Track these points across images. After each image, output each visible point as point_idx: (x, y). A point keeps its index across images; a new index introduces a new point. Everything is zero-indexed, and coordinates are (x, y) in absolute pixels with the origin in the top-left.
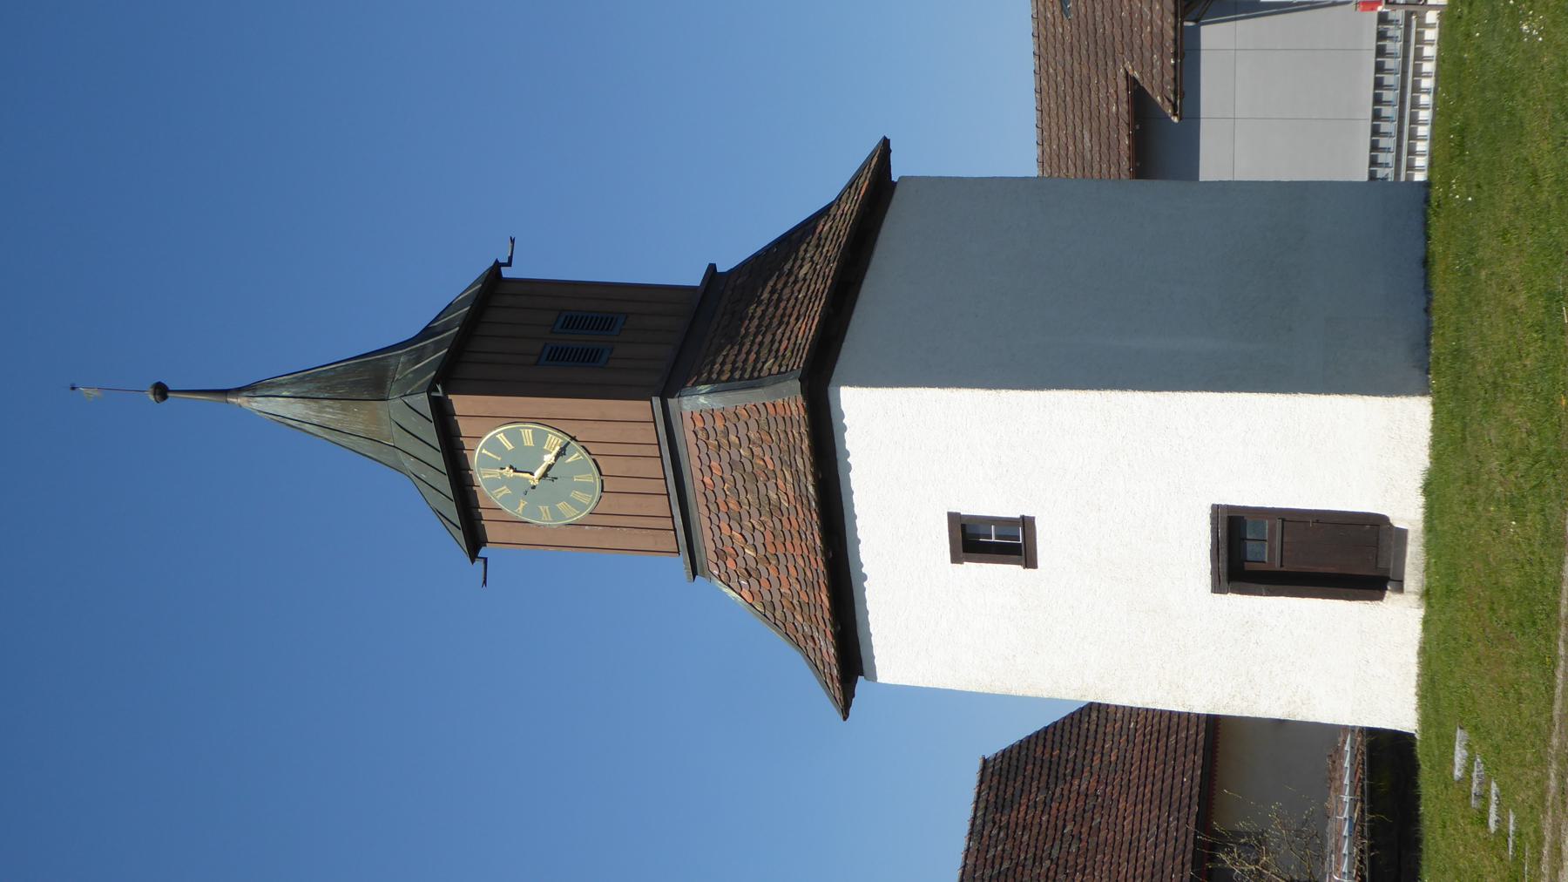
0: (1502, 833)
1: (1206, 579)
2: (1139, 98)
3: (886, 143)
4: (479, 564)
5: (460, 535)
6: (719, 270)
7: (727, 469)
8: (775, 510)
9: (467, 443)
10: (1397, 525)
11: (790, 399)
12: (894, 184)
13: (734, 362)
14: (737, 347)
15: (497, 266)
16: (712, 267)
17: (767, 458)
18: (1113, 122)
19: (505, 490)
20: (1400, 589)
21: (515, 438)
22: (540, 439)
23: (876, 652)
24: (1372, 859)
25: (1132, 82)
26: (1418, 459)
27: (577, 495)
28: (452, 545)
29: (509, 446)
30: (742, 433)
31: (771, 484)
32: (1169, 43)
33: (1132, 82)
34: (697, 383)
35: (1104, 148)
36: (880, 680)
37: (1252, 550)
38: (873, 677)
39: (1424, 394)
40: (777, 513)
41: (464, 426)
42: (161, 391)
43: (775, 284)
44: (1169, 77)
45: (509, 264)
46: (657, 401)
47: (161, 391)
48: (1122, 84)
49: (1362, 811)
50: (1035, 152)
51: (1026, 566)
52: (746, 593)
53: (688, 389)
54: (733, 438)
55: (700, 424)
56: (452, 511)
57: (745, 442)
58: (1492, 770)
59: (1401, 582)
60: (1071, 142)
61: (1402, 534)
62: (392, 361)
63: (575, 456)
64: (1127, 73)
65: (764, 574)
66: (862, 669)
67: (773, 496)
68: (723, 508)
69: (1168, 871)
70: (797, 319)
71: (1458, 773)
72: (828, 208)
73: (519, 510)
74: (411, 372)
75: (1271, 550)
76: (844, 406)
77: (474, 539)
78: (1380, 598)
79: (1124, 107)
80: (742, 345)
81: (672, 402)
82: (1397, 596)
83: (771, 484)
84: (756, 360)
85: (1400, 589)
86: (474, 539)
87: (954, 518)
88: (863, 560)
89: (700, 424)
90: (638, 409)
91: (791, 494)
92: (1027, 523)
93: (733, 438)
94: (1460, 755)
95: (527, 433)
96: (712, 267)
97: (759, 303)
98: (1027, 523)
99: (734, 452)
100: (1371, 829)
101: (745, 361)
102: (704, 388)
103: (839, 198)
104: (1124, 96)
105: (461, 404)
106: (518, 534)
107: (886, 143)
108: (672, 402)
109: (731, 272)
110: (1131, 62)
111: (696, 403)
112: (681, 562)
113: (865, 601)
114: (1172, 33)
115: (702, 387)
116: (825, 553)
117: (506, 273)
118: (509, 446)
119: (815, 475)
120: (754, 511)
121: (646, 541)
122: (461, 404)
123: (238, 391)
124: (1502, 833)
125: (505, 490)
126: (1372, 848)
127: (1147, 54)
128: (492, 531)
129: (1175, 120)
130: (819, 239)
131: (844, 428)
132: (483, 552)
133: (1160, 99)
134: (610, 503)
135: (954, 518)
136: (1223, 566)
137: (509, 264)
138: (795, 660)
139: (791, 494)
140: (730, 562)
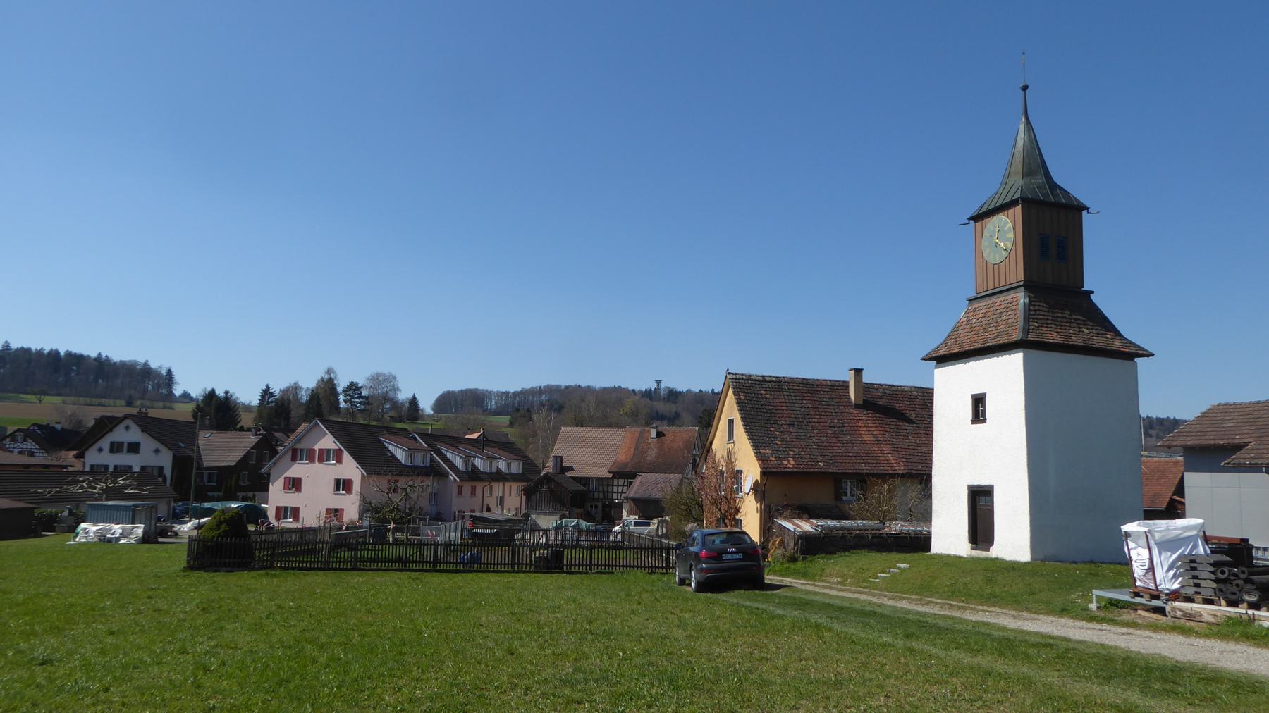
0: (878, 577)
1: (972, 483)
2: (1239, 447)
3: (1152, 355)
4: (967, 221)
5: (976, 213)
6: (1092, 295)
7: (1000, 311)
8: (986, 330)
9: (1006, 213)
10: (991, 548)
11: (1016, 336)
12: (1133, 360)
13: (1039, 310)
14: (1047, 310)
15: (1087, 209)
16: (1092, 292)
17: (1002, 326)
18: (1233, 437)
19: (992, 228)
20: (972, 549)
21: (1008, 231)
22: (1008, 240)
23: (943, 369)
24: (906, 538)
25: (1246, 445)
26: (1009, 556)
27: (992, 256)
28: (972, 211)
29: (1006, 229)
30: (1011, 317)
31: (994, 328)
32: (1256, 461)
33: (1246, 445)
34: (1030, 297)
35: (1222, 433)
36: (936, 370)
37: (983, 498)
38: (937, 367)
39: (1032, 559)
40: (985, 331)
41: (1011, 211)
42: (1025, 88)
43: (1079, 319)
44: (1242, 461)
45: (1088, 213)
46: (1022, 283)
47: (1025, 88)
48: (1246, 441)
49: (925, 535)
50: (1154, 415)
51: (972, 421)
52: (962, 320)
53: (1027, 293)
54: (1009, 313)
55: (1015, 300)
56: (984, 210)
57: (1008, 318)
58: (894, 576)
59: (976, 549)
60: (1231, 418)
61: (988, 550)
62: (1040, 177)
63: (1005, 254)
64: (1250, 442)
65: (967, 327)
66: (941, 363)
67: (990, 329)
68: (988, 310)
69: (923, 465)
70: (1057, 332)
71: (898, 565)
72: (1120, 335)
73: (986, 234)
74: (454, 479)
75: (983, 505)
76: (1017, 354)
77: (978, 217)
78: (970, 542)
79: (1237, 441)
80: (1048, 312)
81: (1022, 289)
82: (970, 548)
83: (994, 328)
84: (1038, 319)
85: (972, 549)
86: (978, 217)
87: (984, 395)
88: (1004, 356)
89: (1015, 300)
90: (1021, 277)
91: (989, 336)
92: (984, 421)
93: (1009, 313)
94: (902, 566)
95: (1011, 235)
96: (1092, 292)
97: (1071, 315)
98: (984, 421)
99: (1005, 314)
100: (917, 537)
101: (1039, 314)
102: (1027, 301)
103: (1125, 339)
104: (1242, 441)
105: (1019, 209)
106: (979, 234)
107: (1152, 355)
108: (1022, 289)
109: (1091, 300)
110: (1255, 445)
111: (1021, 298)
112: (973, 295)
113: (952, 365)
114: (1260, 462)
115: (1028, 299)
116: (969, 350)
117: (1084, 212)
118: (1006, 229)
119: (992, 346)
120: (986, 322)
121: (979, 281)
122: (1019, 209)
123: (1027, 118)
124: (878, 577)
125: (992, 228)
126: (910, 537)
127: (1254, 452)
128: (979, 224)
129: (1222, 464)
130: (1102, 334)
131: (1010, 355)
132: (972, 222)
133: (1236, 458)
134: (990, 267)
135: (984, 395)
136: (975, 489)
137: (1088, 213)
138: (940, 340)
139: (989, 336)
140: (972, 314)
